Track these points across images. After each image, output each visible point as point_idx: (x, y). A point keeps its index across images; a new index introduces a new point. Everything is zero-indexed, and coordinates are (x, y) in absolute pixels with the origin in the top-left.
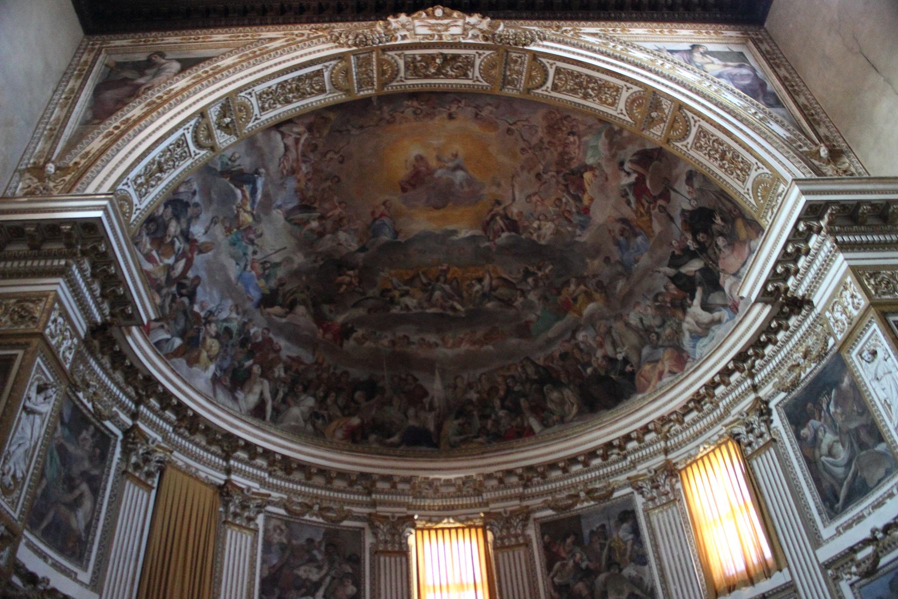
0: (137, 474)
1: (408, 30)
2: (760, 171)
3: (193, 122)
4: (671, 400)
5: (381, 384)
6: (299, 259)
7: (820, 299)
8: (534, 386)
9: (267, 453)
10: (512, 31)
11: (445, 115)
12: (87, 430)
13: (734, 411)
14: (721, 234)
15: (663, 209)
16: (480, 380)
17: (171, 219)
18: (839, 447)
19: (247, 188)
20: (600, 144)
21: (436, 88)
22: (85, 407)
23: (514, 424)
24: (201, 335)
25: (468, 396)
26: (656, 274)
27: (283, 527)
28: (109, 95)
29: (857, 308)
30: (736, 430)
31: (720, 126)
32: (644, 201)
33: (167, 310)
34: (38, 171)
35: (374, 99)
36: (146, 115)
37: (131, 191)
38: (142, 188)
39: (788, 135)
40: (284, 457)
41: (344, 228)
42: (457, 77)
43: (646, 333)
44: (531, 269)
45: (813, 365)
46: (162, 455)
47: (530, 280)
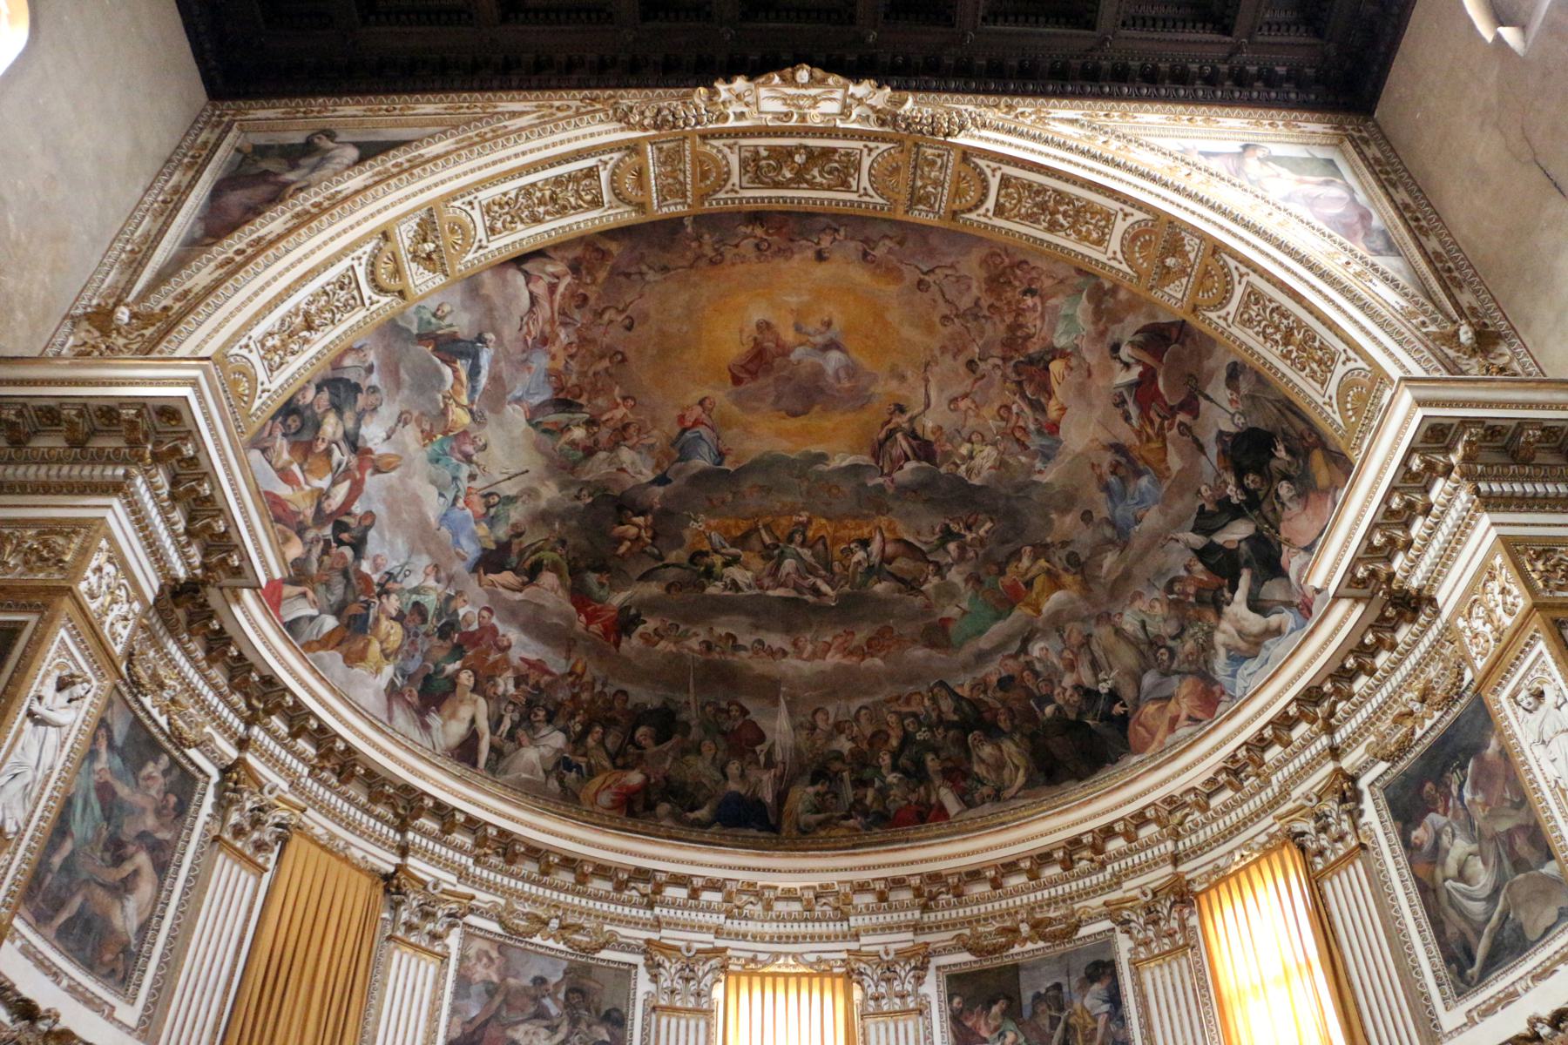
0: (239, 845)
1: (747, 105)
2: (1351, 365)
3: (368, 248)
4: (1187, 768)
5: (684, 716)
6: (550, 492)
7: (1448, 595)
8: (951, 733)
9: (472, 825)
10: (927, 111)
11: (810, 254)
12: (156, 762)
13: (1296, 793)
14: (1286, 477)
15: (1185, 429)
16: (857, 718)
17: (327, 411)
18: (1477, 865)
19: (463, 366)
20: (1079, 313)
21: (795, 207)
22: (155, 721)
23: (913, 797)
24: (372, 612)
25: (835, 746)
26: (1172, 543)
27: (494, 954)
28: (236, 198)
29: (1511, 614)
30: (1298, 827)
31: (1283, 283)
32: (1152, 414)
33: (314, 568)
34: (101, 319)
35: (687, 222)
36: (289, 231)
37: (254, 358)
38: (275, 355)
39: (1404, 304)
40: (503, 833)
41: (629, 443)
42: (830, 188)
43: (1150, 647)
44: (954, 527)
45: (1437, 715)
46: (285, 814)
47: (952, 547)
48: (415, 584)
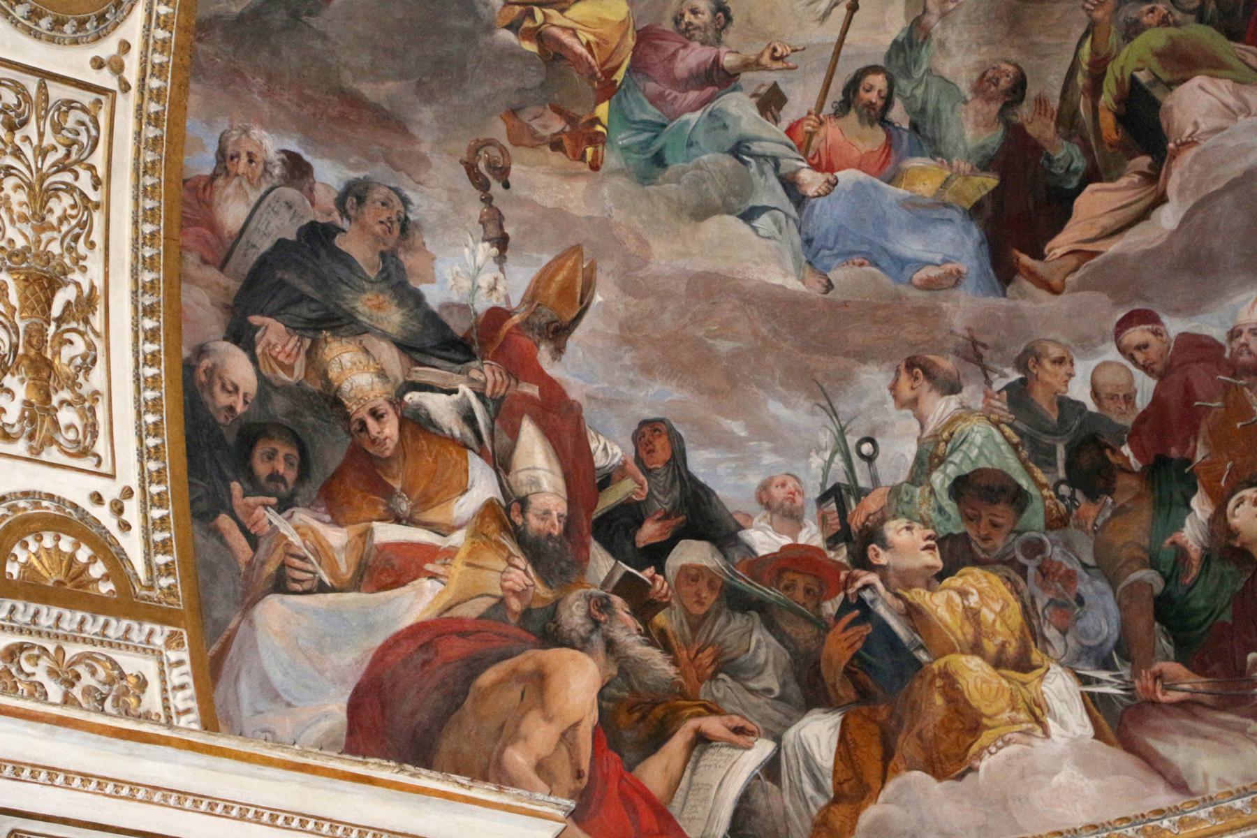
17: (311, 354)
24: (886, 611)
33: (659, 664)
48: (909, 450)
